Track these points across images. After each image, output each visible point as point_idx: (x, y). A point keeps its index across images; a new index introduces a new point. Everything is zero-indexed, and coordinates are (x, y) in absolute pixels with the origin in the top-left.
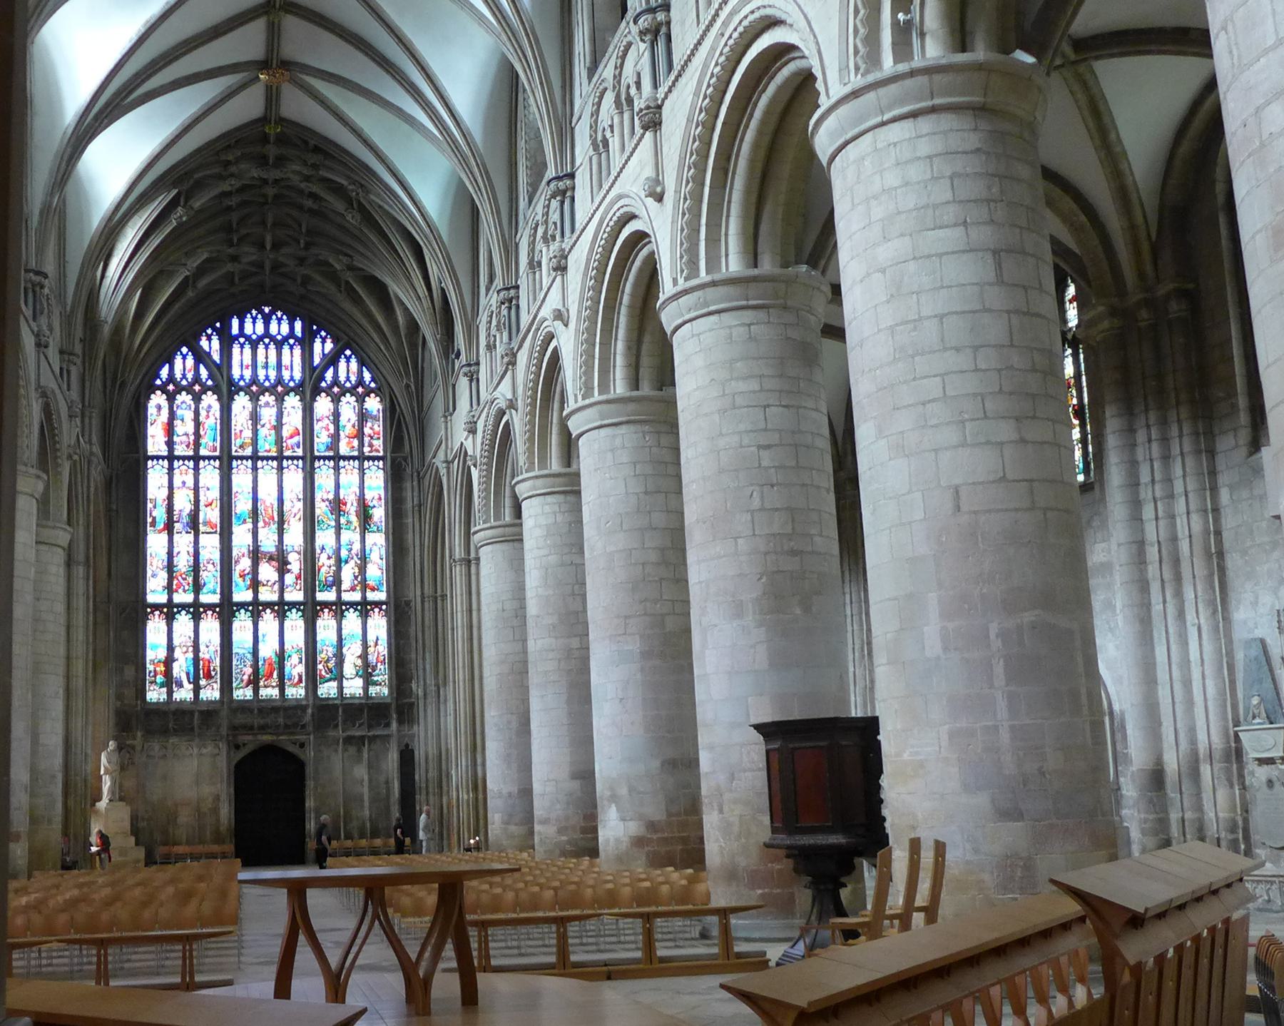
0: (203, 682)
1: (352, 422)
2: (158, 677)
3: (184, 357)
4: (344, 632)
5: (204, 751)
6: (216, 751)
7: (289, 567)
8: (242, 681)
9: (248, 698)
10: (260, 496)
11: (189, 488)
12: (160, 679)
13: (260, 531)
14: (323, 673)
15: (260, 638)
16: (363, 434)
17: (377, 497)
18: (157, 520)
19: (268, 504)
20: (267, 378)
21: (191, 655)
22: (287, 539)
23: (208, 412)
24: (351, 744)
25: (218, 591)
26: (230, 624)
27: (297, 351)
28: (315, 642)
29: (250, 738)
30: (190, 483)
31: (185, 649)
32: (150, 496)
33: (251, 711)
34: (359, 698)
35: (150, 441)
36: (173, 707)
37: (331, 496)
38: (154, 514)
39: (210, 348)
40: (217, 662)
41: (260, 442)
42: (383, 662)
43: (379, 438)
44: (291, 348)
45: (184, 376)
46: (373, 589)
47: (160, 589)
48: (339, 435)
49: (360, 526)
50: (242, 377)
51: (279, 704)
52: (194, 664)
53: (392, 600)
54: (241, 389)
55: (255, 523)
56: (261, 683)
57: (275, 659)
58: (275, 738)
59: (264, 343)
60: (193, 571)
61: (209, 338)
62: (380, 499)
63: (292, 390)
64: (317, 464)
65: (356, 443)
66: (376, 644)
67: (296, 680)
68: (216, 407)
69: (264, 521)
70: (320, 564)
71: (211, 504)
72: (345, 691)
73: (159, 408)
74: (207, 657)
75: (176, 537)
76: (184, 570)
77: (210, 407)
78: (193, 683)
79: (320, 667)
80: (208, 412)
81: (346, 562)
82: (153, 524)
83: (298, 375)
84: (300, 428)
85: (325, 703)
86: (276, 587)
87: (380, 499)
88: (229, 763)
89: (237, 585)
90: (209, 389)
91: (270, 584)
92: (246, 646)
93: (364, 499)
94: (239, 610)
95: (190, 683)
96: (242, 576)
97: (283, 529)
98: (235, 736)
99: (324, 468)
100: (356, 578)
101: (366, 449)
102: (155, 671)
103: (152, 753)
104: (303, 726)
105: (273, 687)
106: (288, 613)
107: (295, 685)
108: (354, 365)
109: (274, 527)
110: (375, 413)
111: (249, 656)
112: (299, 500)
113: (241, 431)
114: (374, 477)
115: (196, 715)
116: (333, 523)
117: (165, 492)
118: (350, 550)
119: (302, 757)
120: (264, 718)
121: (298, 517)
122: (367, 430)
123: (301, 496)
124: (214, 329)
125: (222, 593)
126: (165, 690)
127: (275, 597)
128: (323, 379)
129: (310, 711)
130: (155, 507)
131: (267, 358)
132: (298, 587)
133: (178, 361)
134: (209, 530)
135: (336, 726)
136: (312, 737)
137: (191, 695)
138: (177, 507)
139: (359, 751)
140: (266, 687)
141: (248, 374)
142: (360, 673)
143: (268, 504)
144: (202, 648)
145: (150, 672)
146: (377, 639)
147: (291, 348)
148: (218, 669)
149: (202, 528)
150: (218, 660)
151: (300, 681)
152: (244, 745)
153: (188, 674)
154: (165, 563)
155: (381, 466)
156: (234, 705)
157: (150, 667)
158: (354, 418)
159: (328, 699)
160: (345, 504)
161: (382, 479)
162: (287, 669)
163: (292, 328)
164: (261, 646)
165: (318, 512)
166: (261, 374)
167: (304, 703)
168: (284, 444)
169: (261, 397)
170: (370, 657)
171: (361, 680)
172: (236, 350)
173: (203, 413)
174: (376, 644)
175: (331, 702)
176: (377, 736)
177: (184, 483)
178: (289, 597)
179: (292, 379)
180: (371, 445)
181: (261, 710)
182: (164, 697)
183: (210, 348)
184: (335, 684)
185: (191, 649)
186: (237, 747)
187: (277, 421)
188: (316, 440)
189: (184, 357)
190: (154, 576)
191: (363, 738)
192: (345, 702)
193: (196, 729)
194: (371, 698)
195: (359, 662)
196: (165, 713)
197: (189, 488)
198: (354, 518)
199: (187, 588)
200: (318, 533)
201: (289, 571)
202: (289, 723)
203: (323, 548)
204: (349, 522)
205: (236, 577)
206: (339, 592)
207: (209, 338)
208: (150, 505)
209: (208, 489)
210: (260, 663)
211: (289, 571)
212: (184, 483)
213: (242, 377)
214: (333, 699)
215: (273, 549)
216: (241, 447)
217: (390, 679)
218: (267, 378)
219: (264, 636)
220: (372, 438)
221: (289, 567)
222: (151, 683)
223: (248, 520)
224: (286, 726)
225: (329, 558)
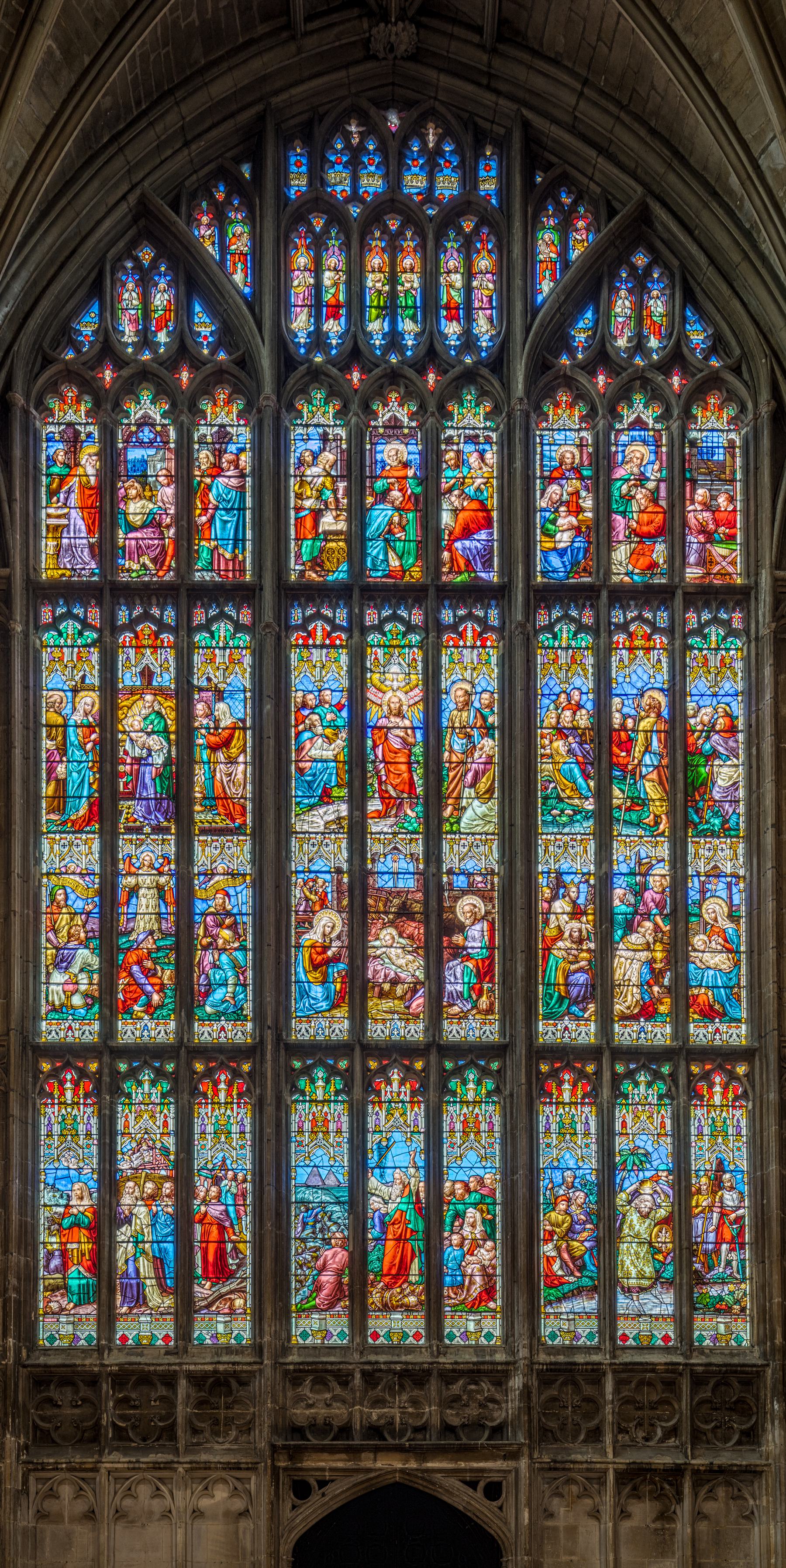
0: (203, 1290)
1: (651, 485)
2: (73, 1271)
3: (145, 285)
4: (621, 1143)
5: (205, 1503)
6: (238, 1504)
7: (458, 939)
8: (318, 1288)
9: (335, 1341)
10: (373, 714)
11: (160, 692)
12: (76, 1278)
13: (376, 826)
14: (556, 1267)
15: (373, 1159)
16: (685, 524)
17: (721, 723)
18: (71, 790)
19: (396, 744)
20: (394, 339)
21: (167, 1206)
22: (450, 858)
23: (219, 454)
24: (636, 1494)
25: (248, 1009)
26: (282, 1110)
27: (483, 262)
28: (533, 1173)
29: (339, 1462)
30: (166, 679)
31: (150, 1185)
32: (48, 716)
33: (343, 1378)
34: (667, 1350)
35: (48, 545)
36: (113, 1360)
37: (583, 720)
38: (61, 769)
39: (224, 249)
40: (245, 1229)
41: (375, 549)
42: (737, 1243)
43: (731, 538)
44: (468, 250)
45: (145, 340)
46: (709, 1013)
47: (77, 1000)
48: (610, 528)
49: (671, 813)
50: (318, 339)
51: (425, 1358)
52: (176, 1232)
53: (772, 1041)
54: (316, 375)
55: (358, 801)
56: (375, 1297)
57: (417, 1224)
58: (413, 1465)
59: (385, 230)
60: (177, 947)
61: (220, 221)
62: (732, 730)
63: (469, 377)
64: (542, 619)
65: (660, 551)
66: (717, 1185)
67: (476, 1290)
68: (243, 435)
69: (384, 798)
70: (551, 932)
71: (226, 743)
72: (624, 1327)
73: (74, 442)
74: (215, 1211)
75: (125, 847)
76: (149, 944)
77: (223, 436)
78: (175, 1292)
79: (548, 1249)
80: (219, 454)
81: (630, 927)
82: (61, 799)
83: (482, 326)
84: (493, 503)
85: (561, 1358)
86: (418, 1003)
87: (732, 730)
88: (275, 1537)
89: (304, 994)
90: (219, 376)
91: (399, 990)
92: (331, 1182)
93: (687, 731)
94: (307, 1071)
95: (163, 1289)
96: (319, 965)
97: (441, 821)
98: (295, 1453)
99: (565, 631)
100: (656, 976)
101: (693, 573)
102: (64, 1254)
103: (50, 1505)
104: (498, 1430)
105: (408, 1309)
106: (454, 1084)
107: (473, 1306)
108: (657, 307)
109: (412, 814)
110: (719, 456)
111: (338, 1212)
112: (488, 730)
113: (317, 515)
114: (714, 661)
115: (183, 1383)
116: (589, 805)
117: (89, 700)
118: (639, 891)
119: (494, 1526)
120: (378, 1402)
121: (483, 785)
122: (696, 515)
123: (493, 719)
124: (236, 186)
125: (259, 1017)
126: (90, 1309)
127: (416, 1032)
128: (565, 344)
129: (517, 1382)
130: (63, 750)
131: (393, 280)
132: (484, 1002)
133: (130, 297)
134: (221, 822)
135: (595, 1435)
136: (524, 1463)
137: (167, 1328)
138: (130, 749)
139: (665, 1516)
140: (387, 1308)
141: (333, 328)
142: (669, 1272)
143: (396, 744)
144: (202, 1186)
145: (50, 1255)
146: (720, 1168)
147: (468, 250)
148: (247, 1250)
149: (202, 817)
150: (247, 1220)
151: (489, 1292)
152: (322, 1484)
153: (158, 1262)
154: (94, 924)
155: (737, 624)
156: (293, 1358)
157: (50, 1241)
158: (653, 472)
159: (572, 1349)
160: (628, 745)
161: (739, 665)
162: (451, 1254)
163: (469, 179)
164: (373, 1182)
165: (545, 768)
166: (376, 326)
167: (500, 1357)
168: (446, 555)
169: (376, 406)
170: (698, 1223)
171: (669, 1298)
172: (302, 259)
173: (204, 457)
174: (717, 1185)
175: (580, 1358)
176: (722, 1470)
177: (147, 674)
178: (452, 1031)
179: (469, 341)
180: (705, 561)
181: (371, 1377)
182: (88, 1332)
183: (224, 249)
184: (590, 1304)
185: (168, 1187)
186: (302, 1490)
187: (422, 481)
188: (542, 543)
189: (145, 285)
190: (62, 962)
191: (675, 1473)
192: (626, 1358)
193: (183, 1436)
194: (701, 1351)
195: (665, 1237)
196: (93, 1381)
197: (160, 692)
198: (651, 789)
199: (156, 998)
200: (546, 836)
201: (458, 952)
202: (455, 1421)
203: (559, 884)
204: (638, 803)
205: (301, 969)
206: (606, 1019)
207: (220, 221)
208: (47, 744)
209: (220, 695)
210: (374, 1233)
211: (458, 952)
212: (147, 674)
213: (318, 339)
214: (588, 1350)
215: (410, 883)
216: (316, 563)
217: (761, 1291)
218: (394, 339)
219: (384, 1151)
220: (710, 537)
221: (458, 939)
222: (54, 1289)
223: (336, 792)
224: (448, 1429)
225: (577, 913)
